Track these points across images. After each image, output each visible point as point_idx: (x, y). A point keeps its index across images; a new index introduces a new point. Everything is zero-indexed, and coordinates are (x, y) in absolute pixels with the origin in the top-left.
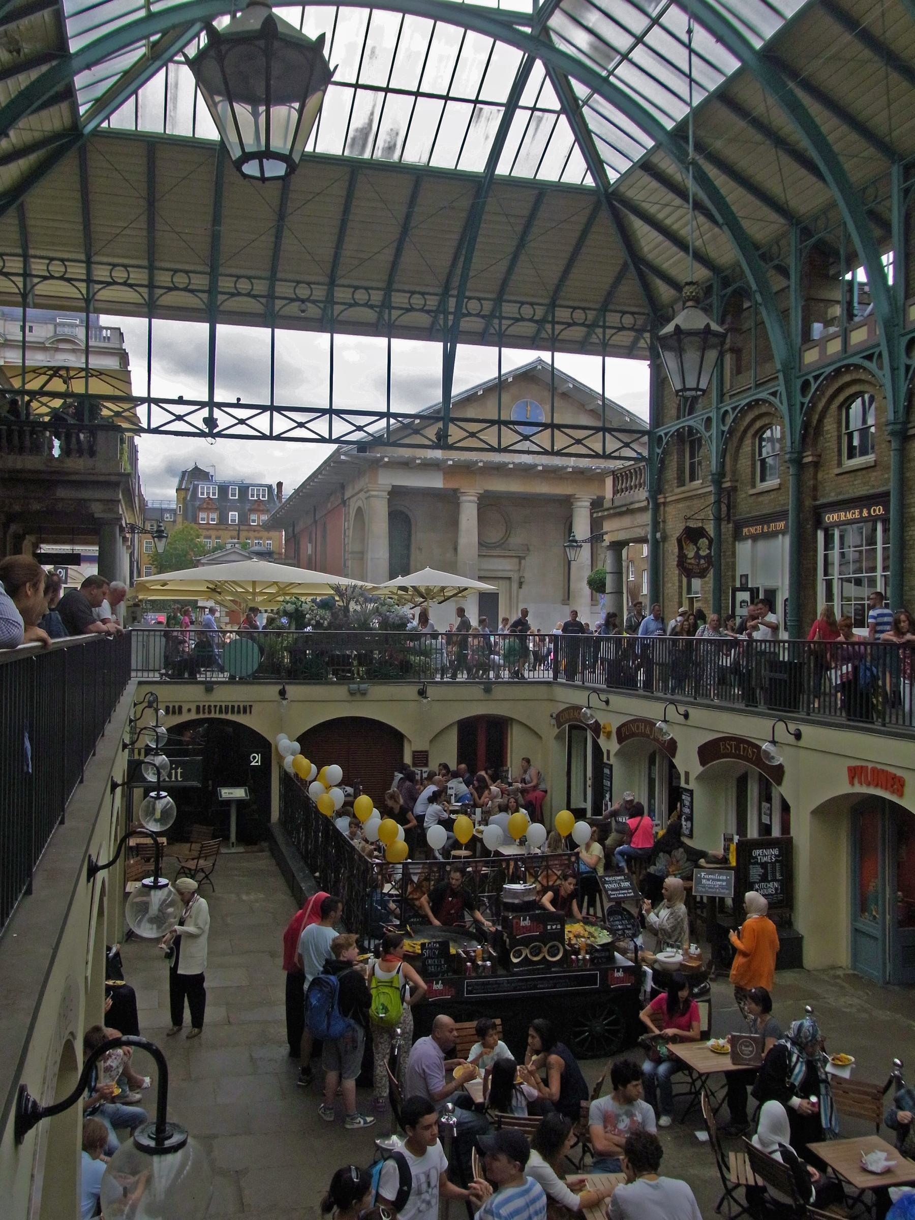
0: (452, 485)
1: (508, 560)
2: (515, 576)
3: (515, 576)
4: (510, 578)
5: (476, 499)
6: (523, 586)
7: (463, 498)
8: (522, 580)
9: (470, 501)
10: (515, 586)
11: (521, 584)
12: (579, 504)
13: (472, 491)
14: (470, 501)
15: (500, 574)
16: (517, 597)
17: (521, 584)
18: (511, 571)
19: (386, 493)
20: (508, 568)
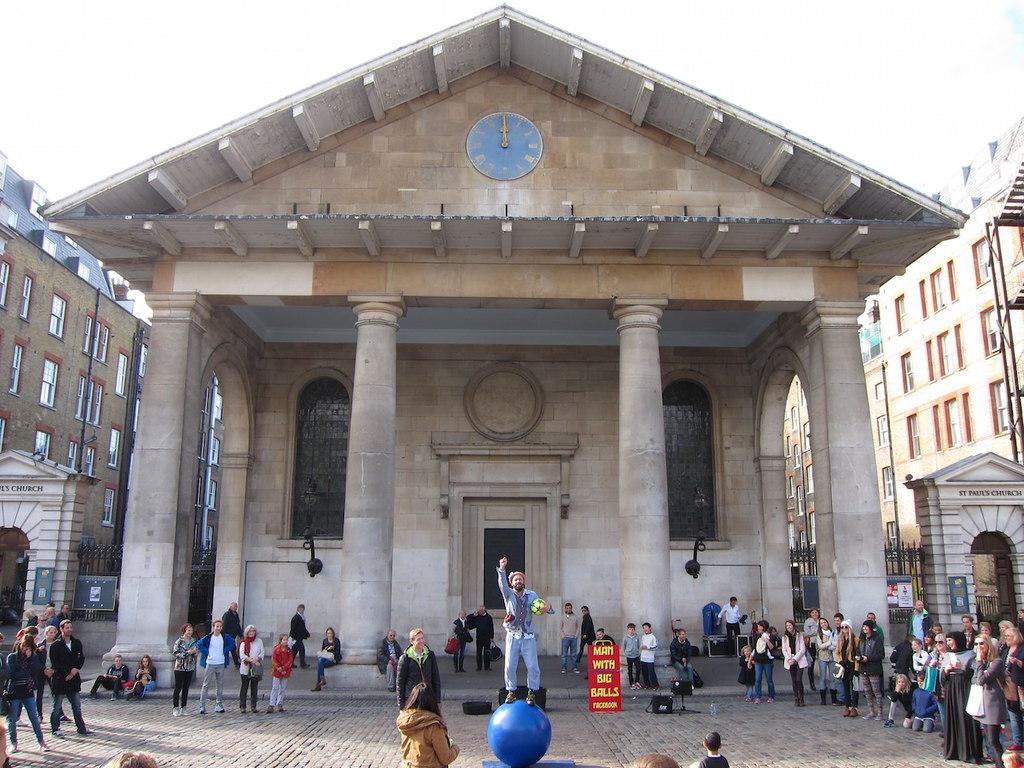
0: (335, 287)
1: (537, 465)
2: (554, 496)
3: (554, 496)
4: (545, 499)
5: (389, 317)
6: (572, 514)
7: (362, 316)
8: (566, 502)
9: (370, 322)
10: (555, 513)
11: (565, 512)
12: (629, 319)
13: (374, 300)
14: (370, 322)
15: (522, 492)
17: (565, 512)
19: (187, 312)
20: (538, 479)
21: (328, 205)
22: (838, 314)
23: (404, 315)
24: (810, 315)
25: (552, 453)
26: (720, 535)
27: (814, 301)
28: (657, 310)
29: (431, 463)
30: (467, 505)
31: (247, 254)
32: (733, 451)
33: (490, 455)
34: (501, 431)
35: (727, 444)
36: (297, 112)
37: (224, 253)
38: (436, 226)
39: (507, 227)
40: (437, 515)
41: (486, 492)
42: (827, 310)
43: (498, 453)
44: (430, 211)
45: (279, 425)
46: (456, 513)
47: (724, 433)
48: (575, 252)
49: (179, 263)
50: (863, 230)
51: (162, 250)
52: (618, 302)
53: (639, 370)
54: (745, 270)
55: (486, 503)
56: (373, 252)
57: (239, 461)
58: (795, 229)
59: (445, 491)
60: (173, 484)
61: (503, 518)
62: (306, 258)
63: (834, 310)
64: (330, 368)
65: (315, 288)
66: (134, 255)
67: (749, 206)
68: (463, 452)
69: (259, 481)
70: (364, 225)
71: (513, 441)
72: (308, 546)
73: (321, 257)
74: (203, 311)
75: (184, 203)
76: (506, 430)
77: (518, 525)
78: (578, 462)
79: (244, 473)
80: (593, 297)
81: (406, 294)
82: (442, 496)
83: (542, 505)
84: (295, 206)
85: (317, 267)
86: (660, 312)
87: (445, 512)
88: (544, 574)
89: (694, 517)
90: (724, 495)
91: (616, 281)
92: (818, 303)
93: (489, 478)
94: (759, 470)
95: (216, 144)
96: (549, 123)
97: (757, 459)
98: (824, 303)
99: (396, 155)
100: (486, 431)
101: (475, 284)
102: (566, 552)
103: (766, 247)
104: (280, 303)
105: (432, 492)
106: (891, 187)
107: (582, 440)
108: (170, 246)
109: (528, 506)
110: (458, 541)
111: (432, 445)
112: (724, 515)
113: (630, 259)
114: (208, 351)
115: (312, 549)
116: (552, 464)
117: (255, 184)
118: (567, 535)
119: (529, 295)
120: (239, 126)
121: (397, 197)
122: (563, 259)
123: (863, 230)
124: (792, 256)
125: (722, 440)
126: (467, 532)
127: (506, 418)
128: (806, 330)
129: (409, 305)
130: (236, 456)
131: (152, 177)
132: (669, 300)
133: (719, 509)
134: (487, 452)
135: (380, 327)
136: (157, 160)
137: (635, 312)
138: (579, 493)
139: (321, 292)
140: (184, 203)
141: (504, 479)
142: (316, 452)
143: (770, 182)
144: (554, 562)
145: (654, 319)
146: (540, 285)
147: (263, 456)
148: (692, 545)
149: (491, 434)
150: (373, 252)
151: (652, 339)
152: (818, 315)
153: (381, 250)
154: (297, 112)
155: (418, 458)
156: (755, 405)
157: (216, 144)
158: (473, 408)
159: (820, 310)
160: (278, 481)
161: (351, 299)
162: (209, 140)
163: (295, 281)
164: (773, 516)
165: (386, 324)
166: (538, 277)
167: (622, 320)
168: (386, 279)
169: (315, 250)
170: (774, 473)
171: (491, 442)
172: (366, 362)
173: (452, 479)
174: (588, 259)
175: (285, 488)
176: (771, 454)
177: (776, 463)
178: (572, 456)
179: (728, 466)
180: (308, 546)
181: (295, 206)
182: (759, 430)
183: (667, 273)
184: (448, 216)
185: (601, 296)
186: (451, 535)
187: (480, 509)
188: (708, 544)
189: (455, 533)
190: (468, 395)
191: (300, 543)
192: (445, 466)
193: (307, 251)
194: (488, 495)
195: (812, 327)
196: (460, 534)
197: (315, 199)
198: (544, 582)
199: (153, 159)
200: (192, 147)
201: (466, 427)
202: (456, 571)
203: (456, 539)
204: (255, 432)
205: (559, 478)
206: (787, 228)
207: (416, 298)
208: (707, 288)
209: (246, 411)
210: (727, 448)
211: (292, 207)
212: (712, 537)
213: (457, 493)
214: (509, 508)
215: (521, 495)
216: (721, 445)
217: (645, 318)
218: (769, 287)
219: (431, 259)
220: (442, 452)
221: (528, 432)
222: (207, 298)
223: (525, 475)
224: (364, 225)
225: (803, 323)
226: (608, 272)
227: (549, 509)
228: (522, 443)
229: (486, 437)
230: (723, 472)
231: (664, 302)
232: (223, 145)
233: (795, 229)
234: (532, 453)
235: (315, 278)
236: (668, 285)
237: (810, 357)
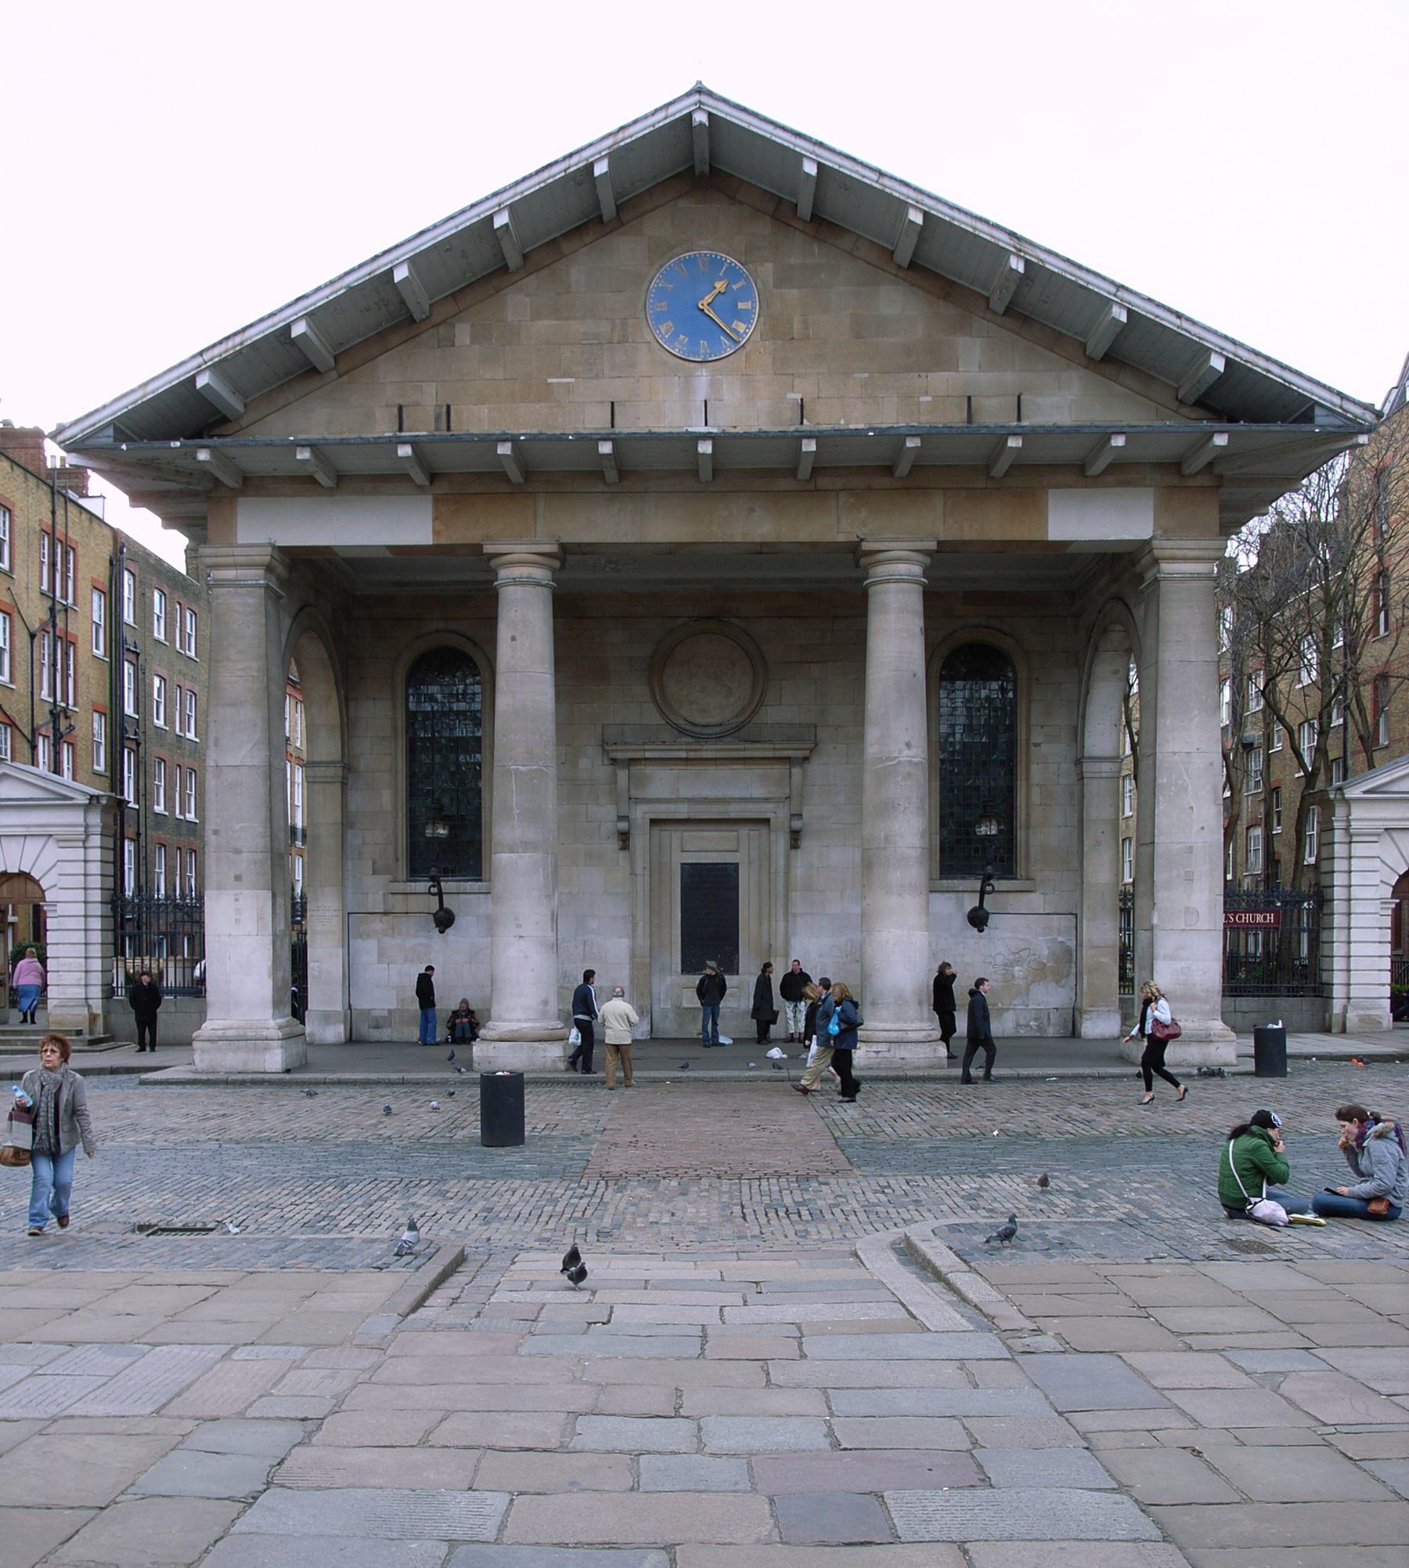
0: (461, 533)
1: (757, 771)
2: (779, 815)
3: (779, 815)
4: (766, 821)
6: (805, 843)
7: (503, 573)
9: (516, 582)
10: (781, 842)
12: (881, 571)
13: (520, 550)
14: (516, 582)
15: (734, 811)
16: (787, 873)
17: (795, 838)
18: (766, 800)
20: (758, 792)
21: (448, 407)
22: (1185, 559)
23: (563, 567)
24: (1146, 560)
25: (778, 754)
26: (1021, 870)
27: (1151, 539)
28: (920, 557)
29: (603, 771)
30: (656, 830)
31: (337, 485)
32: (1044, 748)
33: (687, 759)
34: (704, 722)
35: (1035, 739)
36: (401, 274)
37: (303, 484)
38: (606, 448)
39: (706, 448)
40: (614, 844)
41: (682, 811)
42: (1168, 553)
43: (698, 755)
44: (594, 420)
45: (381, 719)
46: (639, 841)
47: (1034, 721)
48: (804, 472)
49: (241, 499)
50: (1221, 440)
51: (217, 481)
52: (866, 546)
53: (895, 639)
54: (1050, 491)
55: (681, 827)
56: (515, 476)
57: (331, 772)
58: (1119, 441)
59: (624, 811)
60: (262, 813)
61: (708, 848)
62: (421, 490)
63: (1179, 553)
64: (451, 632)
65: (436, 533)
66: (173, 486)
67: (1062, 402)
68: (648, 755)
69: (358, 801)
70: (504, 449)
71: (719, 737)
72: (434, 890)
73: (442, 488)
74: (280, 569)
75: (240, 408)
76: (711, 721)
77: (730, 858)
78: (815, 767)
79: (337, 788)
80: (829, 539)
81: (566, 539)
82: (621, 818)
83: (764, 830)
84: (400, 408)
85: (437, 501)
86: (928, 560)
87: (624, 838)
88: (765, 927)
89: (976, 843)
90: (1028, 814)
91: (863, 514)
92: (1155, 543)
93: (685, 792)
94: (1081, 778)
95: (288, 328)
96: (769, 266)
97: (1079, 762)
98: (1166, 544)
99: (544, 325)
100: (682, 722)
101: (661, 525)
102: (796, 896)
103: (1081, 465)
104: (388, 554)
105: (605, 813)
106: (1268, 371)
107: (822, 733)
108: (229, 481)
109: (744, 831)
110: (643, 882)
111: (603, 744)
112: (1027, 842)
113: (885, 482)
114: (287, 622)
115: (440, 894)
116: (777, 770)
117: (340, 376)
118: (799, 871)
119: (739, 539)
120: (319, 300)
121: (546, 394)
122: (785, 484)
123: (1221, 440)
124: (1121, 473)
125: (1029, 732)
126: (656, 869)
127: (711, 702)
128: (1142, 581)
129: (566, 555)
130: (328, 764)
131: (202, 381)
132: (939, 543)
133: (1021, 835)
134: (683, 755)
135: (530, 588)
136: (207, 356)
137: (890, 561)
138: (812, 811)
139: (443, 541)
140: (240, 408)
141: (707, 792)
142: (438, 758)
143: (1099, 354)
144: (781, 911)
145: (917, 570)
146: (751, 525)
147: (362, 764)
148: (977, 884)
149: (689, 727)
150: (515, 476)
151: (914, 600)
152: (1156, 561)
153: (528, 474)
154: (401, 274)
155: (584, 763)
156: (1080, 681)
157: (288, 328)
158: (662, 690)
159: (1157, 553)
160: (384, 798)
161: (489, 549)
162: (278, 323)
163: (402, 526)
164: (1098, 844)
165: (539, 585)
166: (751, 510)
167: (872, 571)
168: (535, 519)
169: (433, 477)
170: (1103, 782)
171: (690, 740)
172: (513, 639)
173: (634, 793)
174: (825, 482)
175: (396, 808)
176: (1100, 754)
177: (1106, 767)
178: (806, 759)
179: (1036, 771)
180: (434, 890)
181: (400, 408)
182: (1083, 717)
183: (938, 501)
184: (624, 426)
185: (841, 538)
186: (633, 873)
187: (674, 835)
188: (1000, 884)
189: (639, 869)
190: (655, 669)
191: (423, 886)
192: (623, 775)
193: (420, 478)
194: (685, 816)
195: (1149, 576)
196: (647, 872)
197: (429, 397)
198: (765, 939)
199: (201, 353)
200: (254, 335)
201: (652, 716)
202: (641, 924)
203: (640, 879)
204: (347, 729)
205: (787, 791)
206: (1109, 439)
207: (579, 545)
208: (993, 524)
209: (335, 701)
210: (1037, 745)
211: (396, 410)
212: (1009, 873)
213: (641, 814)
214: (715, 834)
215: (733, 816)
216: (1028, 740)
217: (903, 568)
218: (1079, 521)
219: (601, 488)
220: (619, 755)
221: (743, 725)
222: (283, 550)
223: (742, 786)
224: (504, 449)
225: (1138, 569)
226: (851, 501)
227: (773, 836)
228: (739, 738)
229: (682, 732)
230: (1028, 779)
231: (932, 545)
232: (299, 329)
233: (1119, 441)
234: (747, 754)
235: (435, 519)
236: (938, 521)
237: (1146, 614)
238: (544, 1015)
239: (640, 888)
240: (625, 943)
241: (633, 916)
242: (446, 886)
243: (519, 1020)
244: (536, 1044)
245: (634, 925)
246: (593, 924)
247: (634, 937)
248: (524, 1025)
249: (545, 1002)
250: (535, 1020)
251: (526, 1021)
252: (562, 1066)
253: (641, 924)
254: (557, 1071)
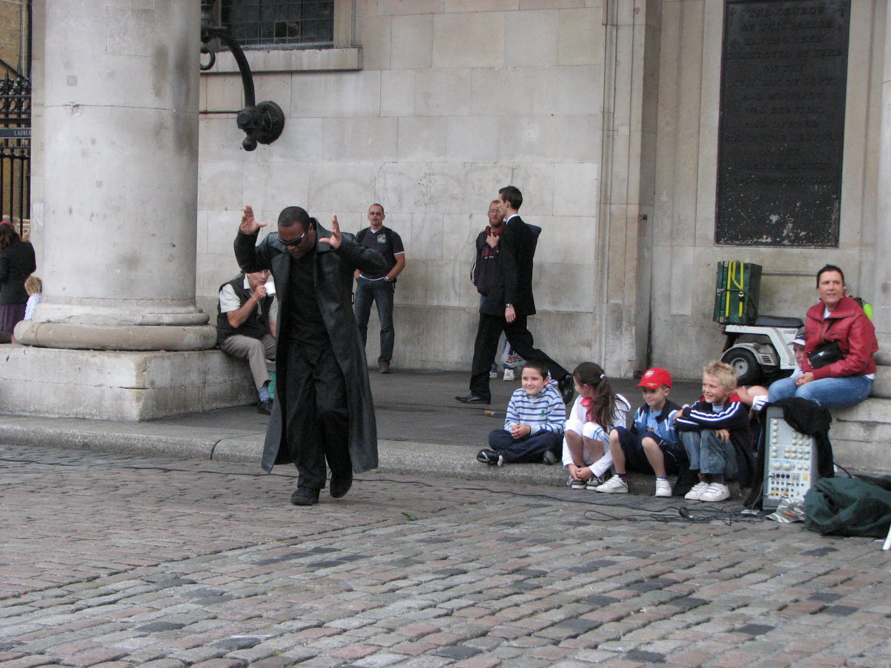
202: (623, 131)
238: (126, 291)
239: (624, 56)
240: (591, 171)
241: (608, 114)
242: (256, 57)
243: (69, 301)
244: (87, 355)
245: (608, 134)
246: (531, 134)
247: (606, 158)
248: (78, 311)
249: (131, 262)
250: (103, 301)
251: (81, 302)
252: (133, 409)
253: (623, 131)
254: (122, 422)
